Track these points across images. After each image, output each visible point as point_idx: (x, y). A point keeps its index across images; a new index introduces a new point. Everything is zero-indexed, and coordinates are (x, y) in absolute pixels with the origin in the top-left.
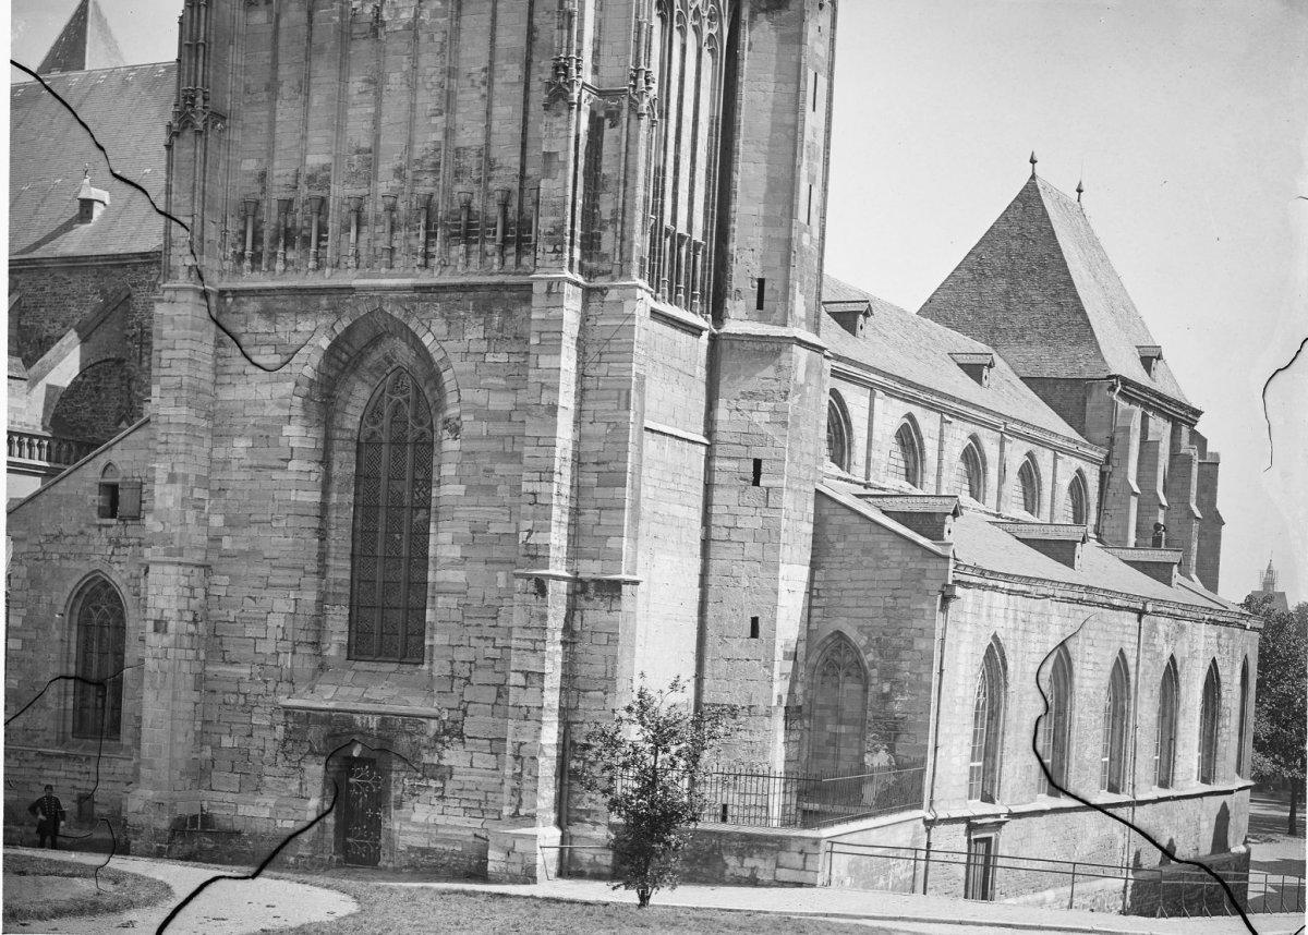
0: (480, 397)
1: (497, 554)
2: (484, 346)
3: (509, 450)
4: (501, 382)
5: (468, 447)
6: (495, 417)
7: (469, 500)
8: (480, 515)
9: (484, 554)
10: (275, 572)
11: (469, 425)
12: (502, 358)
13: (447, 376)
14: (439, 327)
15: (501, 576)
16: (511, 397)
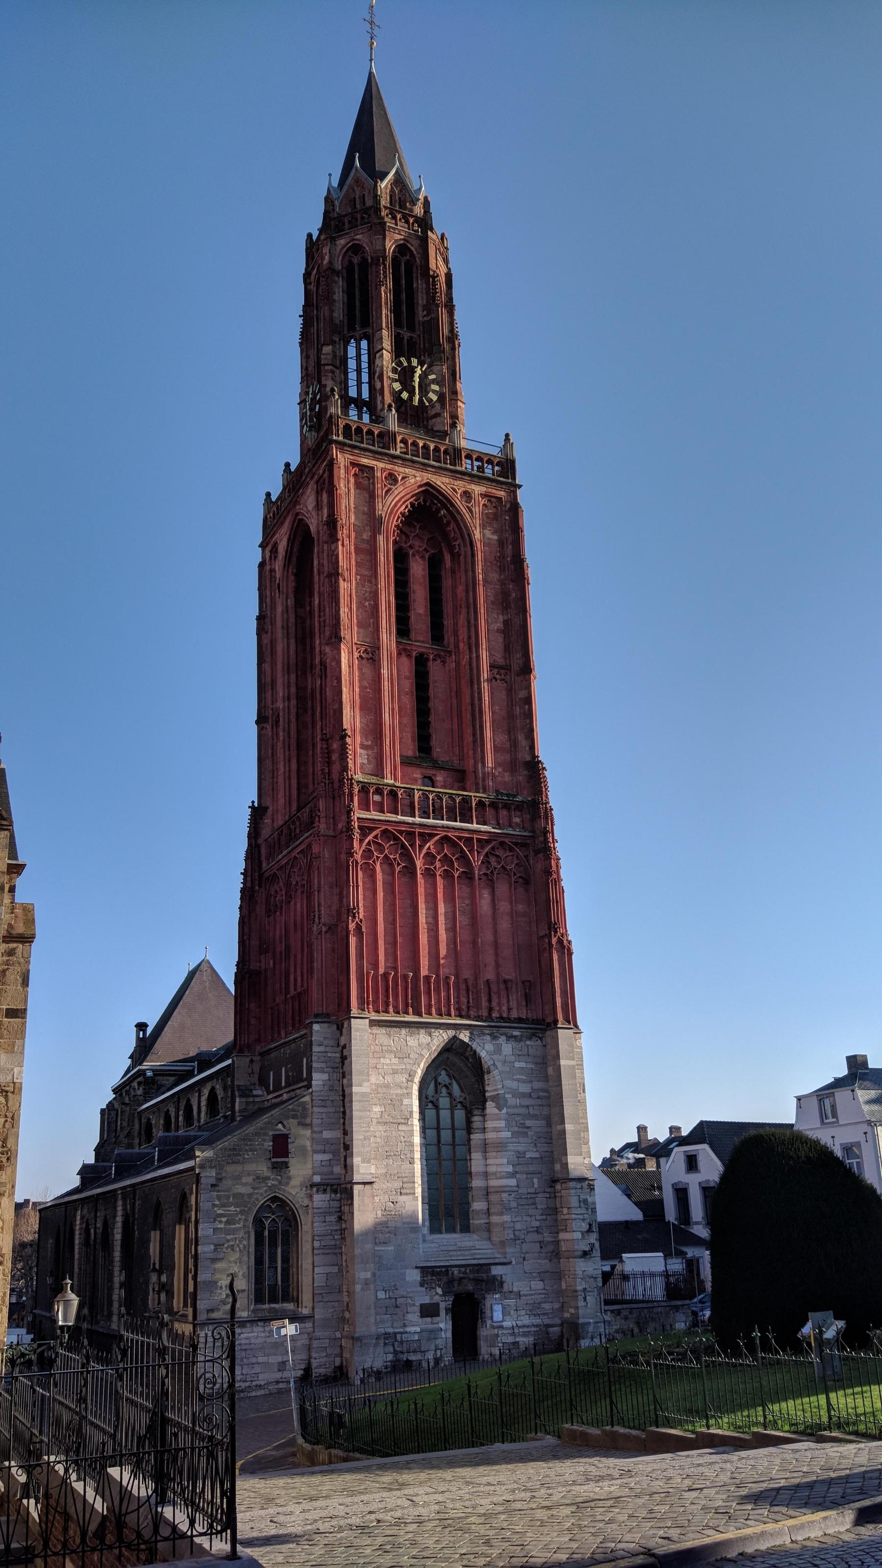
0: (514, 1085)
1: (531, 1168)
2: (513, 1058)
3: (531, 1113)
4: (524, 1077)
5: (511, 1111)
6: (523, 1095)
7: (514, 1140)
8: (520, 1149)
9: (526, 1169)
10: (405, 1185)
11: (511, 1100)
12: (523, 1065)
13: (495, 1072)
14: (489, 1047)
15: (535, 1180)
16: (529, 1085)
